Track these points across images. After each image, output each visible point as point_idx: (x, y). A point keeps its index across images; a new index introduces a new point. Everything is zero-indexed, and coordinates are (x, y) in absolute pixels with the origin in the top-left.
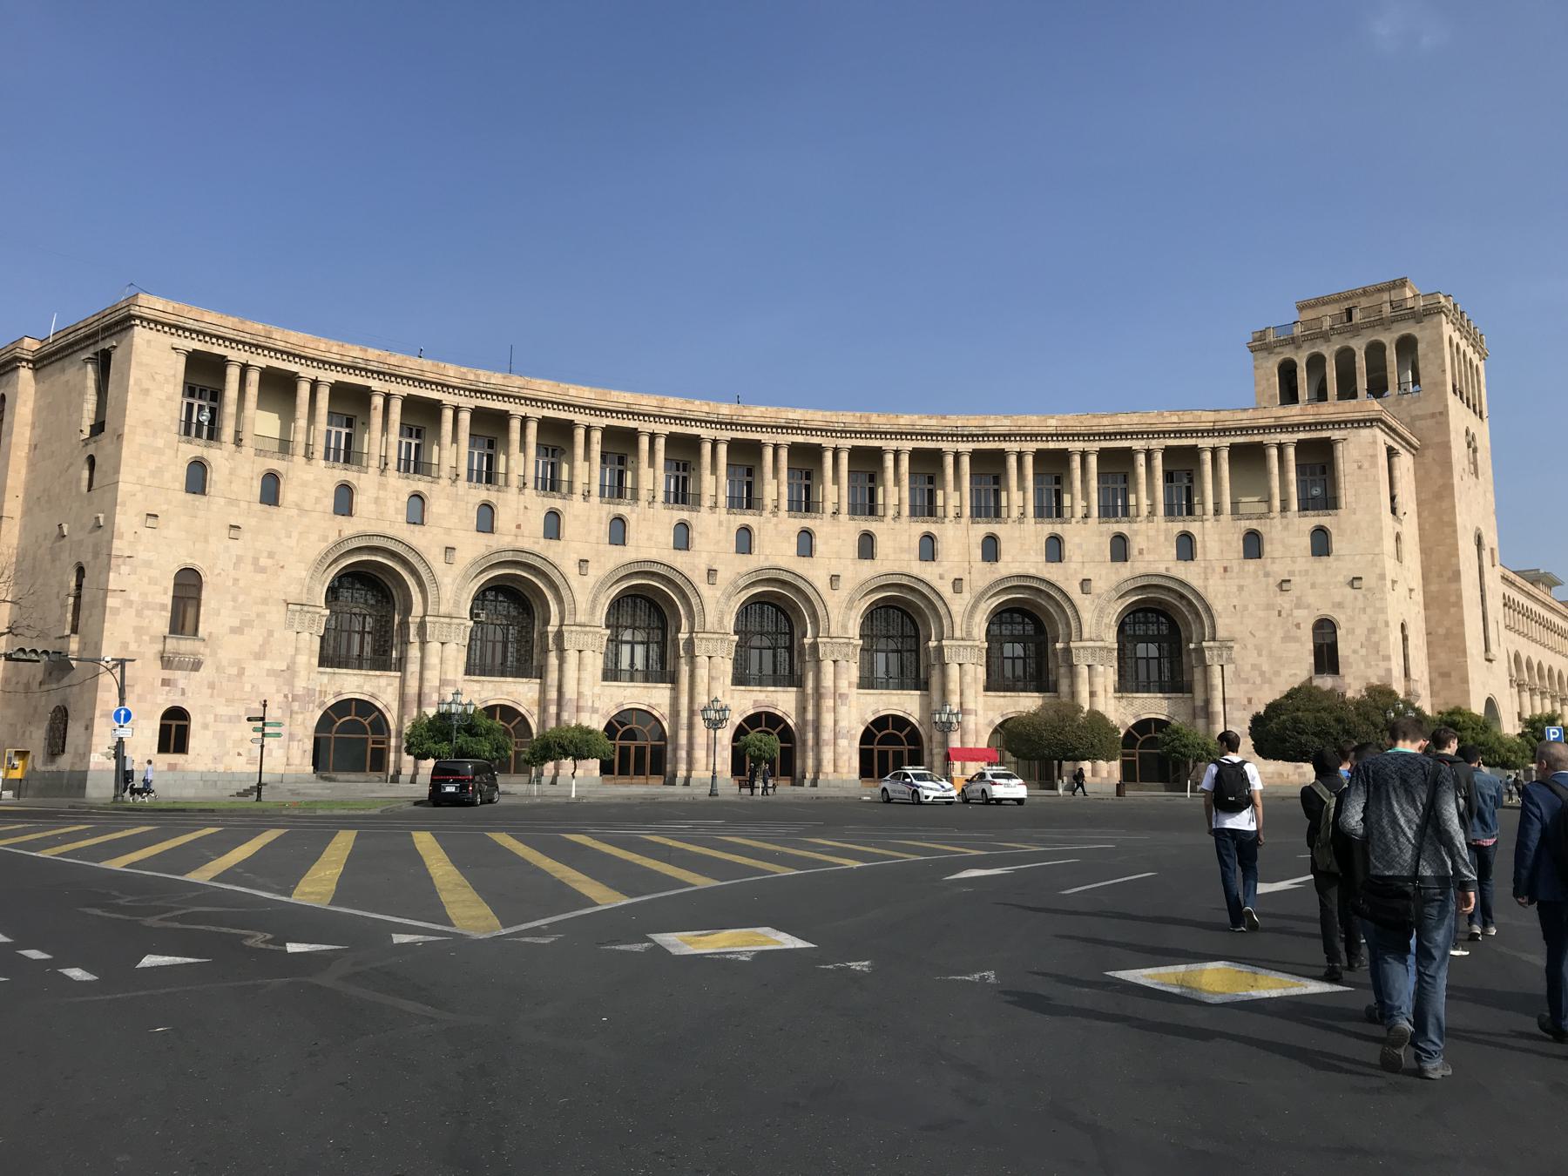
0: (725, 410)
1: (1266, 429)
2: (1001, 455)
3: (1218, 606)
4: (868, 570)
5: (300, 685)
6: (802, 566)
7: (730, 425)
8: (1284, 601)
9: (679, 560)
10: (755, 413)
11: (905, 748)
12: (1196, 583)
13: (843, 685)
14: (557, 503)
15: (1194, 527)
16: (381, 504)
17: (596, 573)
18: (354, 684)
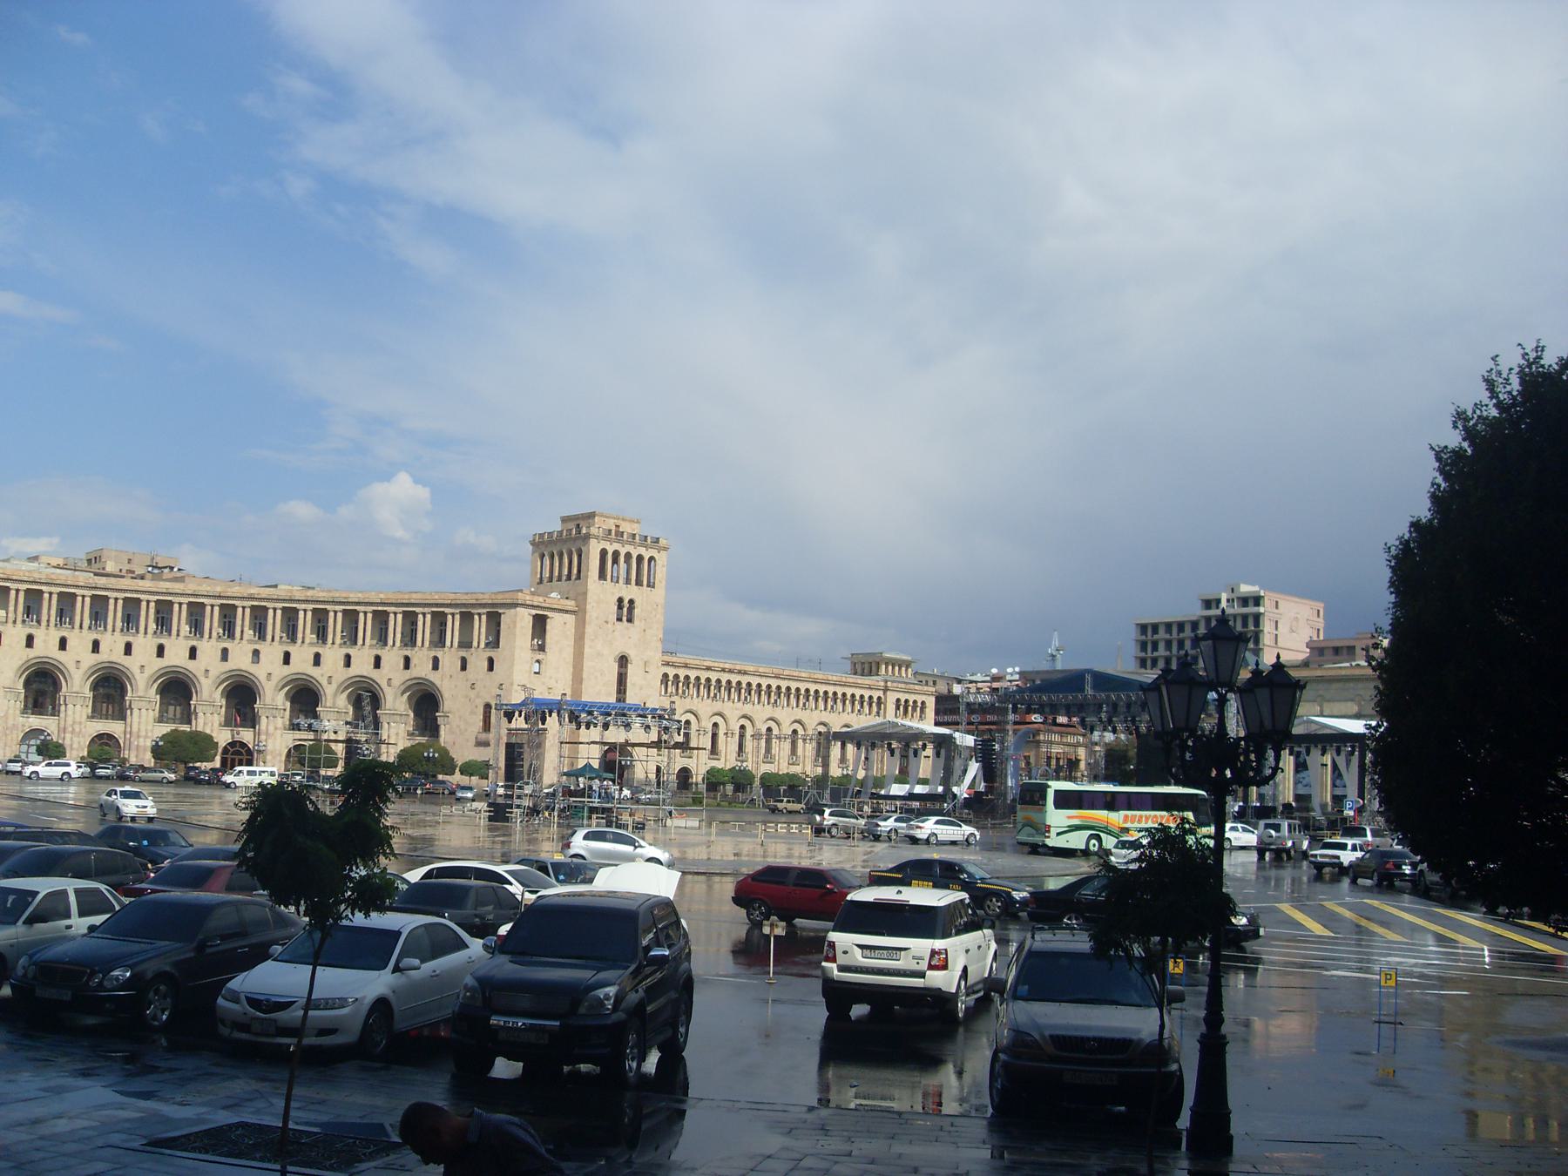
0: (218, 589)
1: (473, 605)
2: (356, 613)
3: (446, 694)
4: (287, 670)
5: (10, 722)
6: (253, 669)
7: (220, 597)
8: (472, 694)
9: (191, 665)
10: (235, 590)
11: (245, 758)
12: (437, 682)
13: (271, 728)
14: (130, 639)
15: (439, 654)
16: (46, 645)
17: (149, 671)
18: (35, 721)
